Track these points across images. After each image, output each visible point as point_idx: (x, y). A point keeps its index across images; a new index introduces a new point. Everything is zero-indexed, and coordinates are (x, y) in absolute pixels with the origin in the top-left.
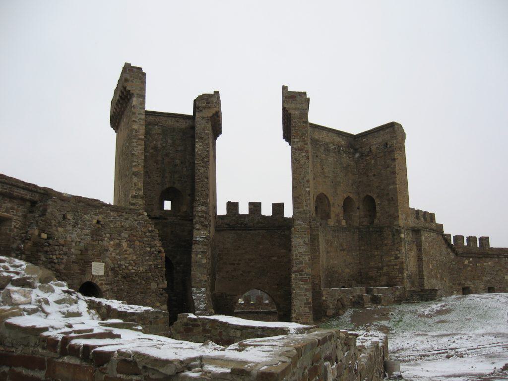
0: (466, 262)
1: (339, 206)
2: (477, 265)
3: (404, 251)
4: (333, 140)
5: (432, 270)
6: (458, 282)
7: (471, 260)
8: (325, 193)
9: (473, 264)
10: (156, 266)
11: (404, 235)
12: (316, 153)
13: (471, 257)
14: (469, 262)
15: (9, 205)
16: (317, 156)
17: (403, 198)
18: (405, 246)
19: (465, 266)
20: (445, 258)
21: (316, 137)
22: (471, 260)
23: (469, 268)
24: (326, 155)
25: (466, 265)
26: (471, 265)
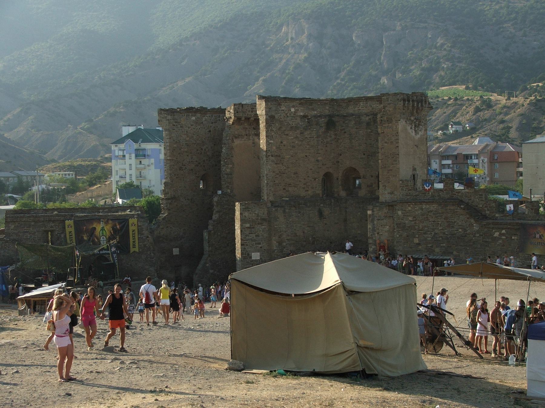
0: (497, 234)
1: (372, 176)
2: (513, 238)
3: (369, 226)
4: (373, 109)
5: (419, 244)
6: (481, 257)
7: (504, 231)
8: (354, 166)
9: (507, 237)
10: (145, 246)
11: (373, 211)
12: (344, 129)
13: (503, 229)
14: (501, 234)
15: (53, 224)
16: (345, 132)
17: (388, 173)
18: (372, 221)
19: (495, 239)
20: (460, 230)
21: (351, 111)
22: (504, 231)
23: (500, 241)
24: (357, 128)
25: (496, 237)
26: (504, 237)
